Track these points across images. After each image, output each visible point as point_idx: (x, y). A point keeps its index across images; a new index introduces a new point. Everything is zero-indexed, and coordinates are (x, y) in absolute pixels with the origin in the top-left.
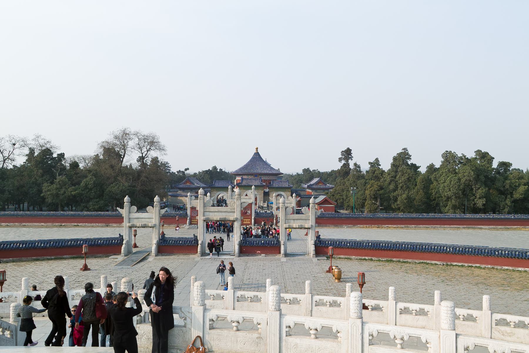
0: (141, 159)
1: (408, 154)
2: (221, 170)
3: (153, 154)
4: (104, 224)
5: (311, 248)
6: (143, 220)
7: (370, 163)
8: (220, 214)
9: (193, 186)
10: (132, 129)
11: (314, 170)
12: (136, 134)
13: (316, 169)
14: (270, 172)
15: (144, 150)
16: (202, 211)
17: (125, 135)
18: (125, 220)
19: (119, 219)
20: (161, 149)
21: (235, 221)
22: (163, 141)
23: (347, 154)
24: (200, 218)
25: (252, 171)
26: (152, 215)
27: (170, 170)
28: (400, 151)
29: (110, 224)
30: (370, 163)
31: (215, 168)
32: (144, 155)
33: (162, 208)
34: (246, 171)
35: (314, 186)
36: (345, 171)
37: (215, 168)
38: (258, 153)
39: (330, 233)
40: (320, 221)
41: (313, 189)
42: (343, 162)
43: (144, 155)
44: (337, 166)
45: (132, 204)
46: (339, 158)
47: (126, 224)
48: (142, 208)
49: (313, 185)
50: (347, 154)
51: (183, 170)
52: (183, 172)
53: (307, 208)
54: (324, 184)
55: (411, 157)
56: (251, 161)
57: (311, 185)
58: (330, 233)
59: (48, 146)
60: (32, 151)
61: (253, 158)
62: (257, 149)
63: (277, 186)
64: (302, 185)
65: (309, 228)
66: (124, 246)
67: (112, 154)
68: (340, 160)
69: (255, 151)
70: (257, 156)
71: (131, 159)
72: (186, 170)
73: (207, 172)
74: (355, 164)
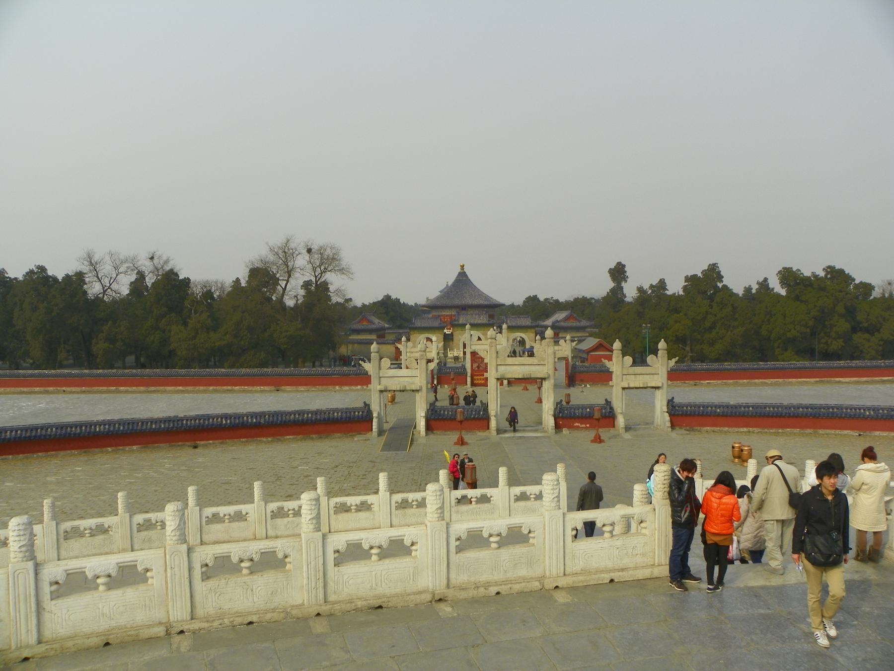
4: (273, 388)
6: (401, 379)
8: (523, 367)
9: (374, 326)
11: (546, 299)
13: (549, 297)
14: (486, 303)
16: (494, 364)
18: (374, 380)
19: (364, 379)
21: (544, 379)
22: (347, 257)
23: (618, 273)
24: (492, 375)
25: (457, 302)
29: (283, 387)
34: (447, 302)
35: (562, 324)
36: (615, 297)
37: (388, 297)
47: (375, 386)
48: (640, 360)
50: (618, 273)
54: (576, 319)
56: (454, 284)
57: (557, 321)
59: (167, 268)
60: (141, 276)
62: (462, 266)
63: (514, 324)
65: (658, 388)
67: (262, 277)
69: (459, 270)
70: (462, 279)
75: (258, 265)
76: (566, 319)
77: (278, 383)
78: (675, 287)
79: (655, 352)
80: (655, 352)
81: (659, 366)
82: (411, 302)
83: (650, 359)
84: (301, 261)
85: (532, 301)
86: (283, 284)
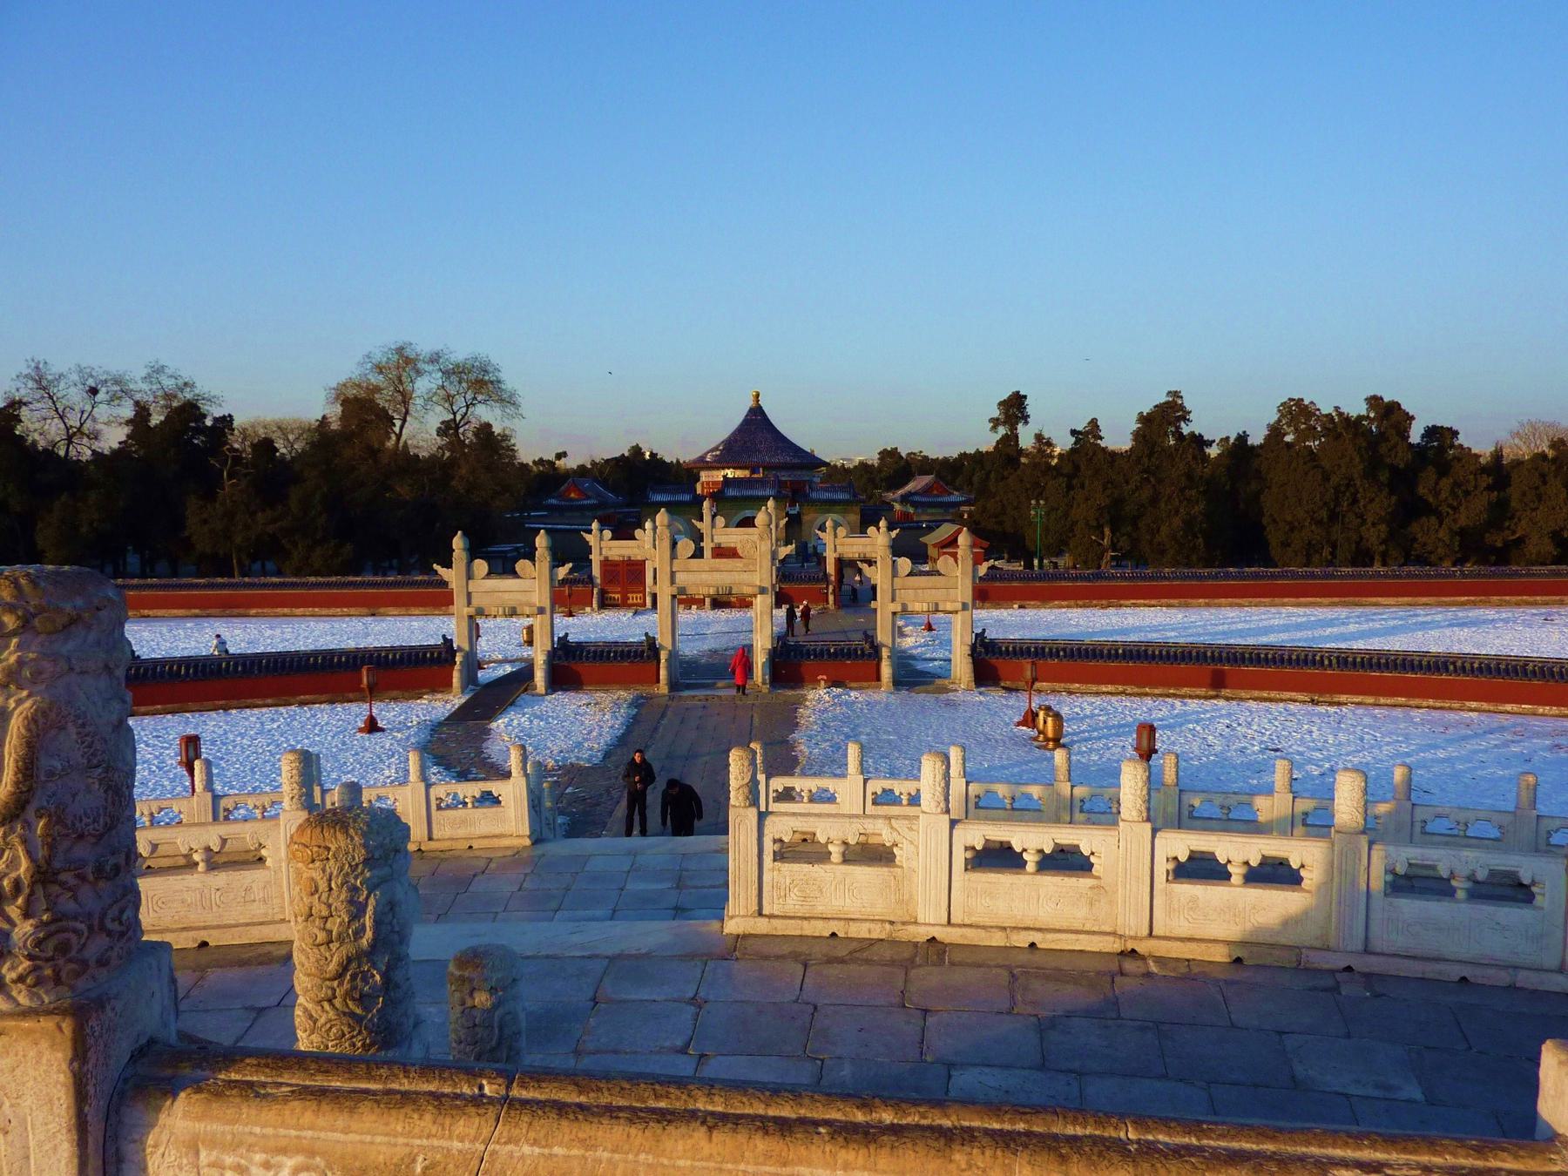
0: (449, 429)
1: (1182, 407)
2: (653, 455)
3: (485, 413)
4: (364, 610)
5: (962, 668)
6: (506, 596)
7: (1073, 432)
10: (423, 345)
12: (434, 359)
14: (796, 461)
15: (460, 403)
17: (405, 363)
20: (507, 401)
22: (510, 380)
23: (1014, 408)
26: (532, 582)
27: (514, 457)
28: (1163, 399)
29: (382, 610)
30: (1073, 432)
31: (637, 451)
32: (458, 417)
33: (557, 561)
35: (917, 498)
37: (637, 451)
38: (760, 408)
39: (1014, 622)
40: (984, 594)
41: (915, 504)
42: (1002, 430)
43: (458, 417)
44: (985, 440)
45: (473, 553)
46: (991, 420)
47: (460, 606)
49: (916, 493)
50: (1014, 408)
51: (552, 457)
52: (552, 463)
53: (951, 560)
55: (1191, 416)
57: (910, 494)
58: (1014, 622)
59: (189, 396)
60: (142, 412)
61: (747, 422)
62: (758, 395)
64: (900, 492)
66: (457, 667)
67: (365, 414)
68: (996, 423)
69: (750, 403)
70: (757, 420)
71: (421, 431)
72: (560, 456)
73: (619, 462)
74: (1039, 437)
75: (351, 393)
76: (927, 491)
77: (373, 607)
78: (1118, 437)
79: (530, 555)
80: (530, 555)
81: (958, 573)
82: (668, 460)
83: (522, 565)
84: (424, 385)
85: (889, 455)
86: (398, 423)
